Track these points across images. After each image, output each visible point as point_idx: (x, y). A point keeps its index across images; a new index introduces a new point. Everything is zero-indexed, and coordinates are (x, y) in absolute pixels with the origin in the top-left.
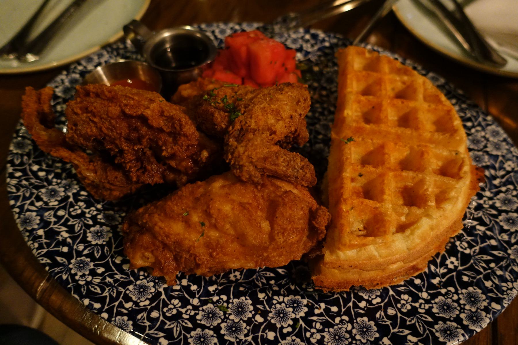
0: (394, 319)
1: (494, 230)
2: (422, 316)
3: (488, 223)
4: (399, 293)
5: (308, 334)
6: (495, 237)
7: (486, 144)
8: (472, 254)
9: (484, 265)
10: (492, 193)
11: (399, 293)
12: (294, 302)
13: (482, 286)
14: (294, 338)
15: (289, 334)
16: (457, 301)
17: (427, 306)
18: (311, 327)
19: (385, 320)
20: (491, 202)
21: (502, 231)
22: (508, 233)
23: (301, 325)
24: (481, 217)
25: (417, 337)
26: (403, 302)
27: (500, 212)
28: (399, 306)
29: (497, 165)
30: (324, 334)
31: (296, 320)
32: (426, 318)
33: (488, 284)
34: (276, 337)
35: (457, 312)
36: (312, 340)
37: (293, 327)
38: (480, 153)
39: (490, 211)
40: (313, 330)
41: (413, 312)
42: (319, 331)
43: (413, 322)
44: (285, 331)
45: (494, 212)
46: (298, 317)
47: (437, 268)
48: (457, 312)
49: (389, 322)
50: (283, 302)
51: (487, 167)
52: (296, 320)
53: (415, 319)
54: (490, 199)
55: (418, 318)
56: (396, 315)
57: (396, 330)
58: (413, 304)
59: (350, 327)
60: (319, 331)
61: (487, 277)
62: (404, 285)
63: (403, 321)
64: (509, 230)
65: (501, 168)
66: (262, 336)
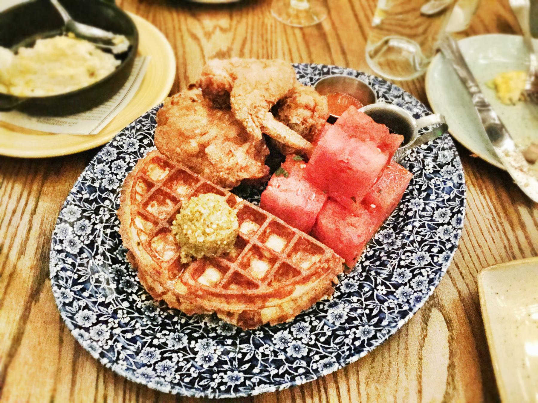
0: (103, 200)
1: (92, 304)
2: (108, 317)
3: (100, 307)
4: (132, 319)
5: (181, 355)
6: (88, 299)
7: (111, 170)
8: (93, 276)
9: (80, 273)
10: (116, 334)
11: (132, 319)
12: (210, 360)
13: (73, 257)
14: (136, 150)
15: (140, 149)
16: (79, 236)
17: (92, 221)
18: (184, 360)
19: (106, 196)
20: (110, 325)
21: (86, 307)
22: (82, 308)
23: (189, 354)
24: (91, 204)
25: (100, 303)
26: (125, 315)
27: (98, 322)
28: (125, 312)
29: (131, 360)
30: (126, 164)
31: (196, 353)
32: (105, 318)
33: (70, 261)
34: (143, 143)
35: (75, 229)
36: (176, 354)
37: (192, 350)
38: (152, 362)
39: (105, 318)
40: (181, 359)
41: (96, 212)
42: (129, 162)
43: (92, 206)
44: (143, 149)
45: (102, 319)
46: (197, 356)
47: (105, 249)
48: (75, 229)
49: (103, 196)
50: (215, 353)
51: (137, 353)
52: (196, 353)
53: (93, 209)
54: (112, 328)
55: (92, 210)
56: (103, 202)
57: (97, 195)
58: (118, 320)
59: (118, 177)
60: (129, 162)
61: (73, 265)
62: (134, 326)
63: (97, 203)
64: (83, 310)
65: (126, 359)
66: (149, 138)
